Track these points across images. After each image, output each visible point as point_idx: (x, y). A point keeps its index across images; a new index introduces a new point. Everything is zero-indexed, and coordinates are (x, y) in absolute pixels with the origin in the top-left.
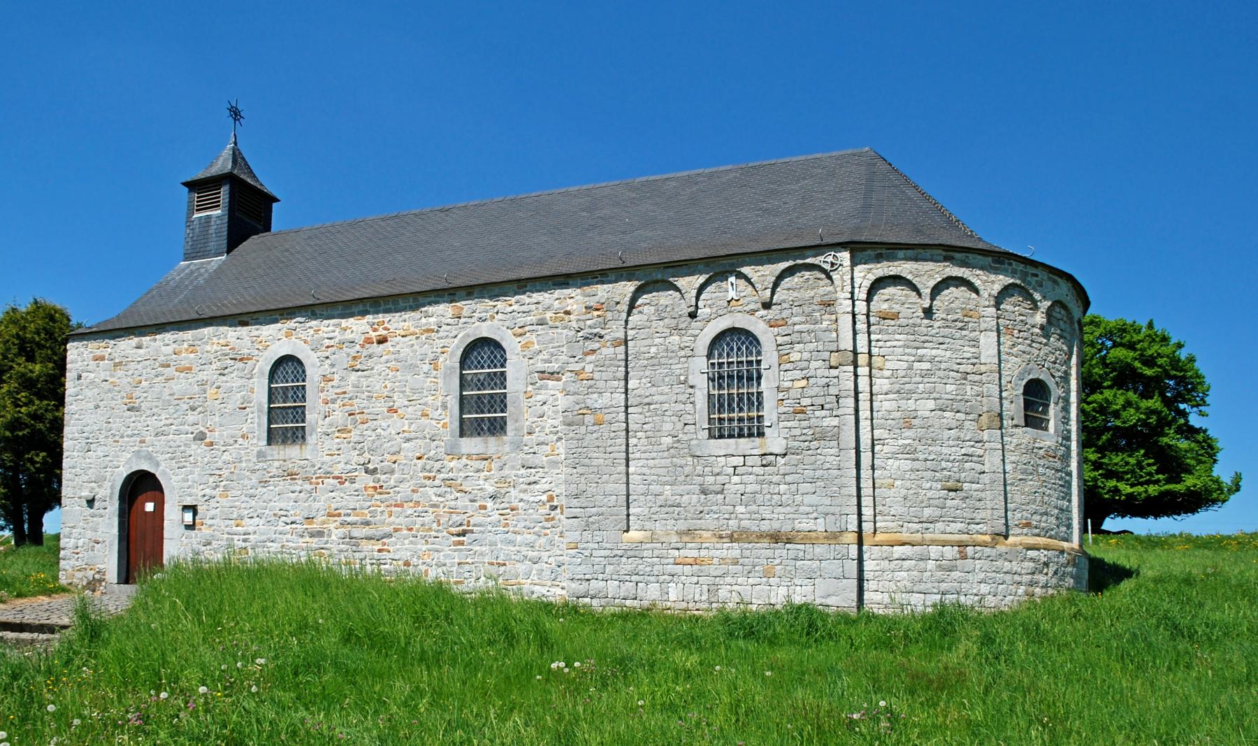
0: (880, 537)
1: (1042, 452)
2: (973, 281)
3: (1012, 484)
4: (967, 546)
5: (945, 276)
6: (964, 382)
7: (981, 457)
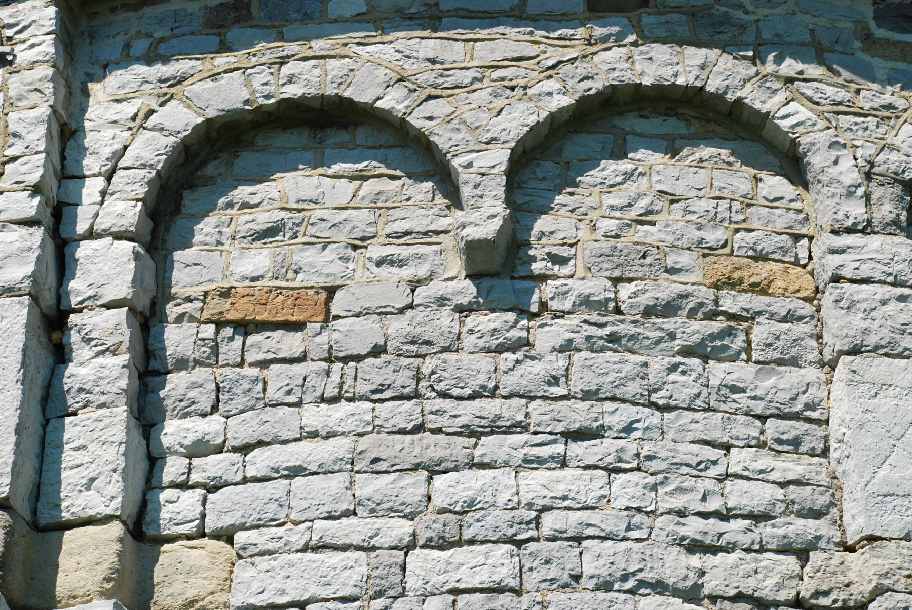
5: (596, 85)
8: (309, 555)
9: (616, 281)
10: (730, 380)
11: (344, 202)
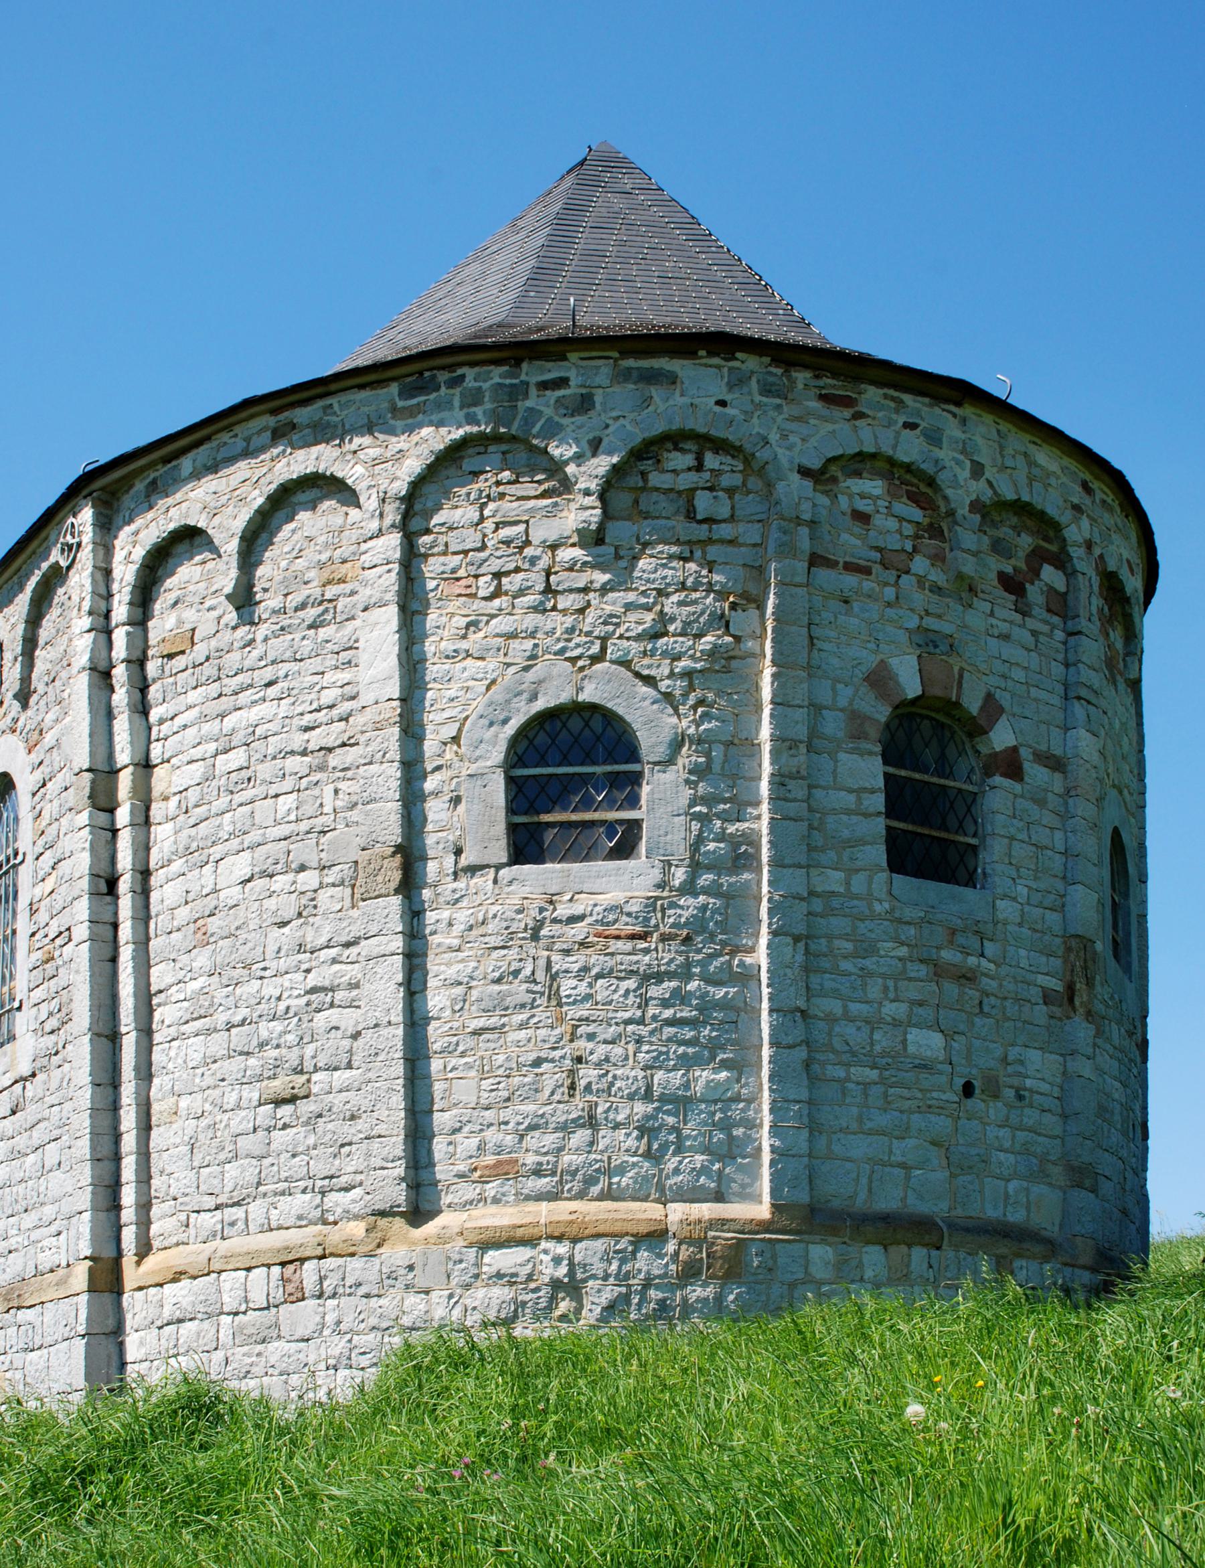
1: (578, 931)
2: (339, 475)
3: (446, 1051)
4: (302, 1260)
5: (274, 486)
7: (357, 986)
9: (286, 595)
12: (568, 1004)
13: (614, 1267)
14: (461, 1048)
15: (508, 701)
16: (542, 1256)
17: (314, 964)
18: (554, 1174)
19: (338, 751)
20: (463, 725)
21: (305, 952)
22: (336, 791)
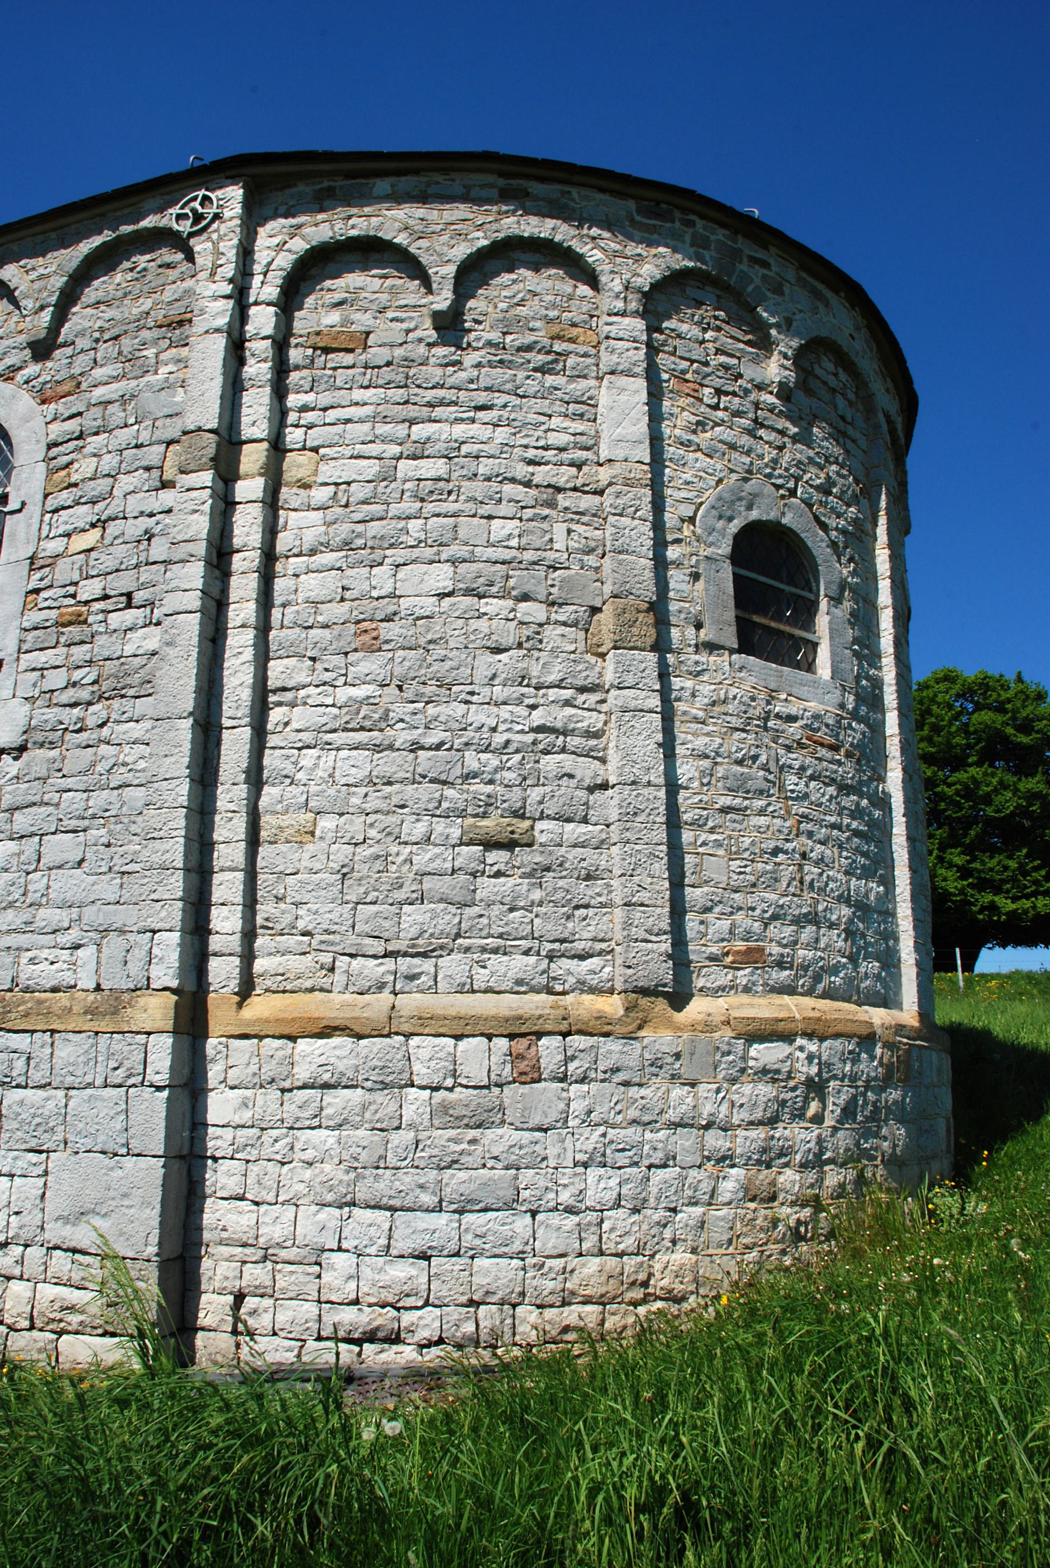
0: (259, 1007)
1: (794, 730)
3: (698, 824)
4: (539, 1035)
5: (501, 235)
6: (546, 511)
7: (597, 735)
8: (353, 461)
9: (504, 334)
10: (555, 384)
11: (376, 289)
12: (792, 799)
13: (848, 1068)
14: (710, 824)
15: (733, 502)
16: (798, 1053)
17: (542, 701)
18: (791, 968)
19: (570, 493)
20: (697, 510)
21: (528, 686)
22: (569, 531)
